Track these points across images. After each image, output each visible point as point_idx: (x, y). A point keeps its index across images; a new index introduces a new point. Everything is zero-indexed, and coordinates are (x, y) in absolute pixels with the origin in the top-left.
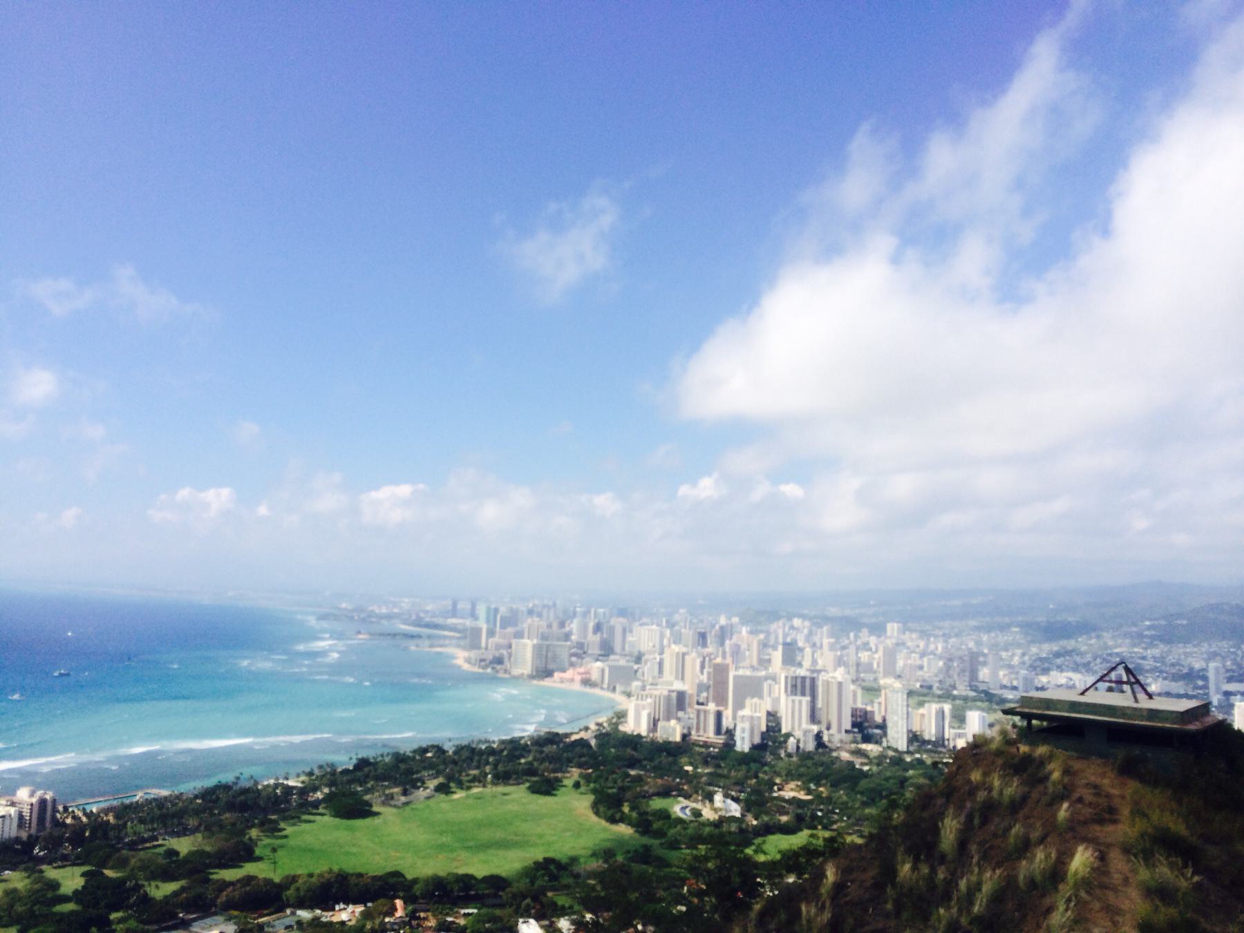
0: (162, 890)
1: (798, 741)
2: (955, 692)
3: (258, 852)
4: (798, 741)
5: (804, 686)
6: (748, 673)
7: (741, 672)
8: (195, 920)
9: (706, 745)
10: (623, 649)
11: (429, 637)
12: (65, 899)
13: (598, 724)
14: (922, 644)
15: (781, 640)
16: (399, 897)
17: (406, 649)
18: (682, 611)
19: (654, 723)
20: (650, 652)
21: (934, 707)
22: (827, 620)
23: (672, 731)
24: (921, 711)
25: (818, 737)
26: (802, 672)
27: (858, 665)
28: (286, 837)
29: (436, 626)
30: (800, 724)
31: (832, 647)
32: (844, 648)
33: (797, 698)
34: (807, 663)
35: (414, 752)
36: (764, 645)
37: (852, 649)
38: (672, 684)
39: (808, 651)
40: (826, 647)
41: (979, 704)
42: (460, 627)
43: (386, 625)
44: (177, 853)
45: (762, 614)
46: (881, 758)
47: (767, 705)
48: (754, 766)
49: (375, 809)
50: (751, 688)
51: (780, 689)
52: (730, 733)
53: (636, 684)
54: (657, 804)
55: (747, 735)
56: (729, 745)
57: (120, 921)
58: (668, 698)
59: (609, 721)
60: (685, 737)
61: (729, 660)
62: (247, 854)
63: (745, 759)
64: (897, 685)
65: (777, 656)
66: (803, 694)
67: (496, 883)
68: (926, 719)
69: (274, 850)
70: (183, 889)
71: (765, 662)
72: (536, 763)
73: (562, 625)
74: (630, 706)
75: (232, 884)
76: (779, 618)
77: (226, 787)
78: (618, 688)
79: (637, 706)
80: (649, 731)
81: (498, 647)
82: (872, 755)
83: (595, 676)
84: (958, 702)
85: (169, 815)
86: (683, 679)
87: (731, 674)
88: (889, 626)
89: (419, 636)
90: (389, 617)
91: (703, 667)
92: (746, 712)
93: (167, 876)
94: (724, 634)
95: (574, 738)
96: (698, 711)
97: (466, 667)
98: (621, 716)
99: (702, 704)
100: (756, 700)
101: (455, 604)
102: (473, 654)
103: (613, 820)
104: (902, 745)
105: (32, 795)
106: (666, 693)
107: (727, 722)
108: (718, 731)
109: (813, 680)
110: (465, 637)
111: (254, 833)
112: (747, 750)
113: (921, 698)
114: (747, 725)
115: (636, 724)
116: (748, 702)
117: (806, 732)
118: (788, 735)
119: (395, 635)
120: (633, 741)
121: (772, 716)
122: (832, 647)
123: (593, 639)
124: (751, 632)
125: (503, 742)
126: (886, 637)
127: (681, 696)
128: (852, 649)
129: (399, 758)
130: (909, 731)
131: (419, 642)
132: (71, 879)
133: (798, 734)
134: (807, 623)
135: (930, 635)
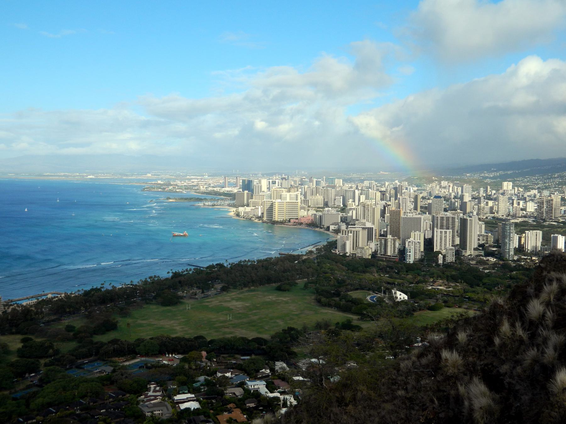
4: (444, 257)
30: (445, 245)
35: (207, 268)
38: (364, 224)
41: (559, 230)
52: (403, 252)
55: (412, 254)
60: (374, 255)
78: (332, 227)
84: (545, 229)
87: (402, 215)
91: (383, 213)
92: (411, 239)
95: (305, 257)
113: (522, 227)
118: (439, 252)
121: (429, 243)
127: (370, 230)
129: (198, 271)
133: (444, 251)
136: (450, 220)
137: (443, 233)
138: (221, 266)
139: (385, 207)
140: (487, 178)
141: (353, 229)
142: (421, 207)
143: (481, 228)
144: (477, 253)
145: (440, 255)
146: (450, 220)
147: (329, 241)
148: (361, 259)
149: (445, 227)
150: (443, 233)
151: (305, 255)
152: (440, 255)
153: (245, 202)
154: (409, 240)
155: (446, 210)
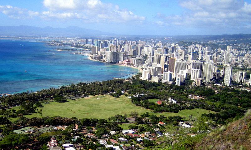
0: (13, 120)
1: (196, 83)
2: (247, 68)
3: (36, 111)
5: (199, 66)
6: (181, 61)
7: (179, 62)
9: (166, 84)
10: (141, 54)
11: (80, 50)
13: (132, 77)
14: (238, 52)
15: (192, 52)
16: (76, 124)
17: (73, 54)
18: (160, 42)
19: (150, 77)
20: (149, 55)
21: (240, 72)
22: (207, 44)
23: (155, 79)
24: (235, 74)
25: (202, 81)
26: (198, 62)
27: (216, 59)
28: (43, 107)
29: (81, 47)
30: (196, 77)
31: (209, 54)
32: (212, 54)
33: (196, 70)
34: (200, 58)
36: (186, 53)
37: (215, 54)
39: (200, 55)
40: (206, 53)
42: (89, 47)
43: (66, 47)
45: (185, 42)
46: (221, 88)
47: (186, 72)
48: (181, 90)
49: (67, 100)
50: (182, 66)
51: (190, 67)
52: (174, 81)
53: (144, 66)
54: (151, 101)
56: (174, 83)
58: (155, 69)
59: (136, 76)
61: (175, 57)
63: (177, 88)
64: (229, 65)
65: (190, 57)
66: (198, 69)
67: (103, 121)
68: (237, 76)
71: (186, 58)
72: (114, 87)
73: (121, 47)
74: (143, 72)
76: (191, 44)
79: (145, 72)
80: (149, 79)
81: (101, 53)
82: (218, 87)
83: (132, 62)
84: (248, 71)
86: (160, 63)
87: (176, 62)
88: (228, 47)
89: (76, 50)
90: (67, 44)
92: (180, 73)
93: (13, 116)
94: (174, 49)
95: (125, 81)
96: (165, 74)
97: (92, 59)
98: (140, 74)
99: (166, 71)
100: (183, 70)
101: (87, 40)
102: (94, 56)
103: (137, 105)
104: (228, 84)
106: (154, 68)
107: (173, 77)
108: (170, 80)
109: (202, 64)
110: (91, 51)
112: (179, 85)
113: (236, 70)
114: (180, 78)
115: (145, 77)
116: (180, 71)
117: (198, 80)
119: (69, 50)
120: (142, 82)
121: (188, 76)
122: (209, 54)
123: (131, 51)
124: (182, 49)
125: (103, 82)
126: (227, 50)
127: (159, 68)
128: (215, 54)
130: (231, 80)
131: (76, 52)
133: (195, 80)
134: (201, 46)
135: (241, 49)
136: (200, 65)
137: (196, 71)
138: (85, 84)
139: (167, 57)
140: (219, 43)
141: (150, 68)
142: (185, 58)
143: (215, 68)
144: (212, 81)
145: (193, 82)
146: (200, 65)
147: (138, 73)
148: (155, 83)
149: (197, 68)
150: (196, 71)
151: (126, 80)
152: (193, 82)
153: (96, 52)
154: (179, 74)
155: (198, 60)
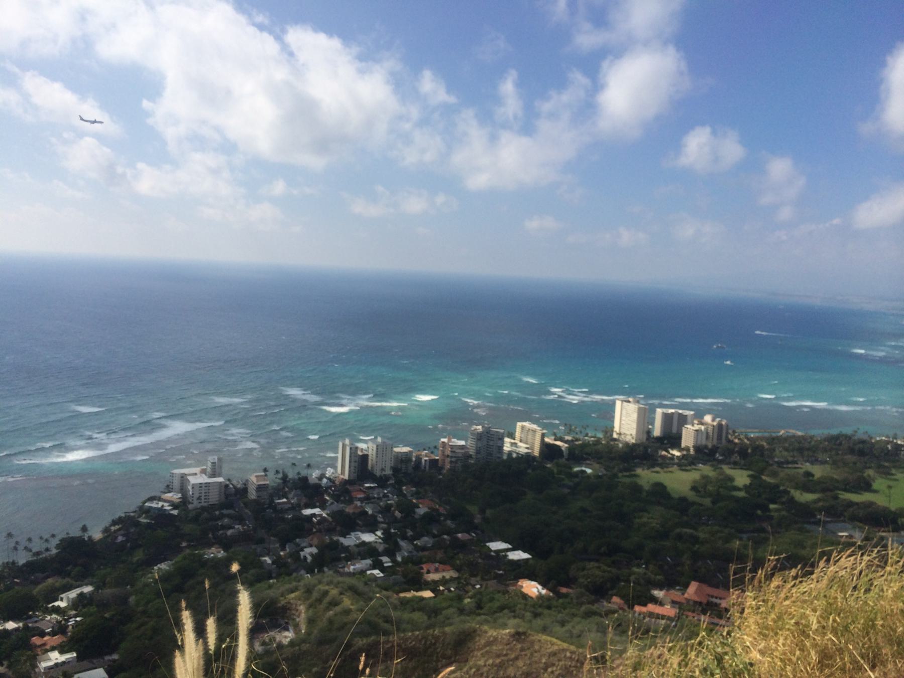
3: (875, 486)
8: (829, 522)
12: (739, 489)
44: (813, 476)
57: (776, 510)
62: (866, 486)
69: (890, 487)
70: (819, 500)
75: (857, 504)
77: (848, 438)
85: (805, 448)
93: (806, 488)
105: (713, 420)
111: (871, 472)
132: (741, 478)
